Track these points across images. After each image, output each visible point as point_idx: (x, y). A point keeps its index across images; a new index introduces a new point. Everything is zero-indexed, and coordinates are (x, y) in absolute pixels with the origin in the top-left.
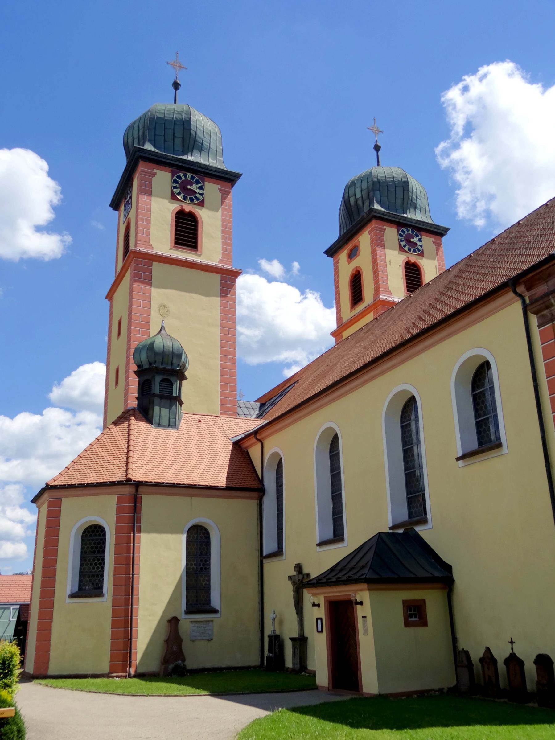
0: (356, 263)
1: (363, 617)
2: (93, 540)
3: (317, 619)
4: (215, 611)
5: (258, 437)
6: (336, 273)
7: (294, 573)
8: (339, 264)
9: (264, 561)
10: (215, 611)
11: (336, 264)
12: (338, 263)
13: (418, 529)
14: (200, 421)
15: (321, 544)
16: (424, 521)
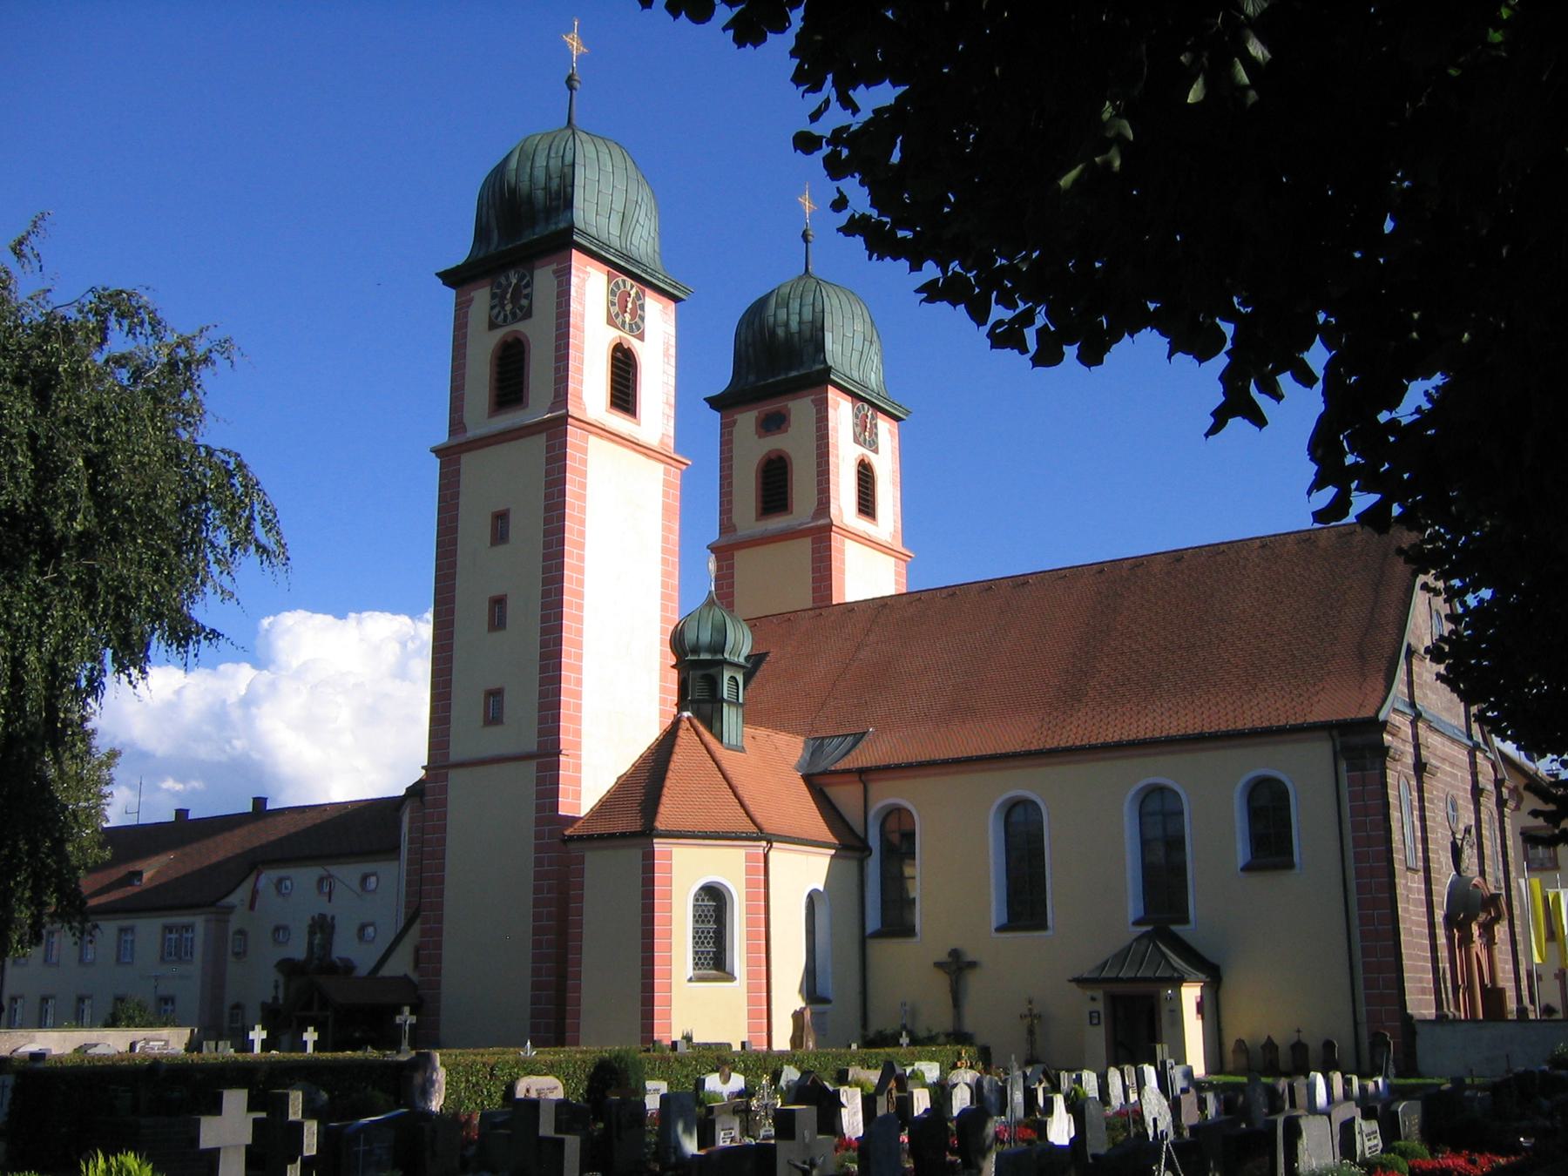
2: (706, 906)
3: (1091, 1013)
7: (950, 960)
8: (736, 430)
11: (727, 429)
15: (999, 929)
16: (1185, 920)
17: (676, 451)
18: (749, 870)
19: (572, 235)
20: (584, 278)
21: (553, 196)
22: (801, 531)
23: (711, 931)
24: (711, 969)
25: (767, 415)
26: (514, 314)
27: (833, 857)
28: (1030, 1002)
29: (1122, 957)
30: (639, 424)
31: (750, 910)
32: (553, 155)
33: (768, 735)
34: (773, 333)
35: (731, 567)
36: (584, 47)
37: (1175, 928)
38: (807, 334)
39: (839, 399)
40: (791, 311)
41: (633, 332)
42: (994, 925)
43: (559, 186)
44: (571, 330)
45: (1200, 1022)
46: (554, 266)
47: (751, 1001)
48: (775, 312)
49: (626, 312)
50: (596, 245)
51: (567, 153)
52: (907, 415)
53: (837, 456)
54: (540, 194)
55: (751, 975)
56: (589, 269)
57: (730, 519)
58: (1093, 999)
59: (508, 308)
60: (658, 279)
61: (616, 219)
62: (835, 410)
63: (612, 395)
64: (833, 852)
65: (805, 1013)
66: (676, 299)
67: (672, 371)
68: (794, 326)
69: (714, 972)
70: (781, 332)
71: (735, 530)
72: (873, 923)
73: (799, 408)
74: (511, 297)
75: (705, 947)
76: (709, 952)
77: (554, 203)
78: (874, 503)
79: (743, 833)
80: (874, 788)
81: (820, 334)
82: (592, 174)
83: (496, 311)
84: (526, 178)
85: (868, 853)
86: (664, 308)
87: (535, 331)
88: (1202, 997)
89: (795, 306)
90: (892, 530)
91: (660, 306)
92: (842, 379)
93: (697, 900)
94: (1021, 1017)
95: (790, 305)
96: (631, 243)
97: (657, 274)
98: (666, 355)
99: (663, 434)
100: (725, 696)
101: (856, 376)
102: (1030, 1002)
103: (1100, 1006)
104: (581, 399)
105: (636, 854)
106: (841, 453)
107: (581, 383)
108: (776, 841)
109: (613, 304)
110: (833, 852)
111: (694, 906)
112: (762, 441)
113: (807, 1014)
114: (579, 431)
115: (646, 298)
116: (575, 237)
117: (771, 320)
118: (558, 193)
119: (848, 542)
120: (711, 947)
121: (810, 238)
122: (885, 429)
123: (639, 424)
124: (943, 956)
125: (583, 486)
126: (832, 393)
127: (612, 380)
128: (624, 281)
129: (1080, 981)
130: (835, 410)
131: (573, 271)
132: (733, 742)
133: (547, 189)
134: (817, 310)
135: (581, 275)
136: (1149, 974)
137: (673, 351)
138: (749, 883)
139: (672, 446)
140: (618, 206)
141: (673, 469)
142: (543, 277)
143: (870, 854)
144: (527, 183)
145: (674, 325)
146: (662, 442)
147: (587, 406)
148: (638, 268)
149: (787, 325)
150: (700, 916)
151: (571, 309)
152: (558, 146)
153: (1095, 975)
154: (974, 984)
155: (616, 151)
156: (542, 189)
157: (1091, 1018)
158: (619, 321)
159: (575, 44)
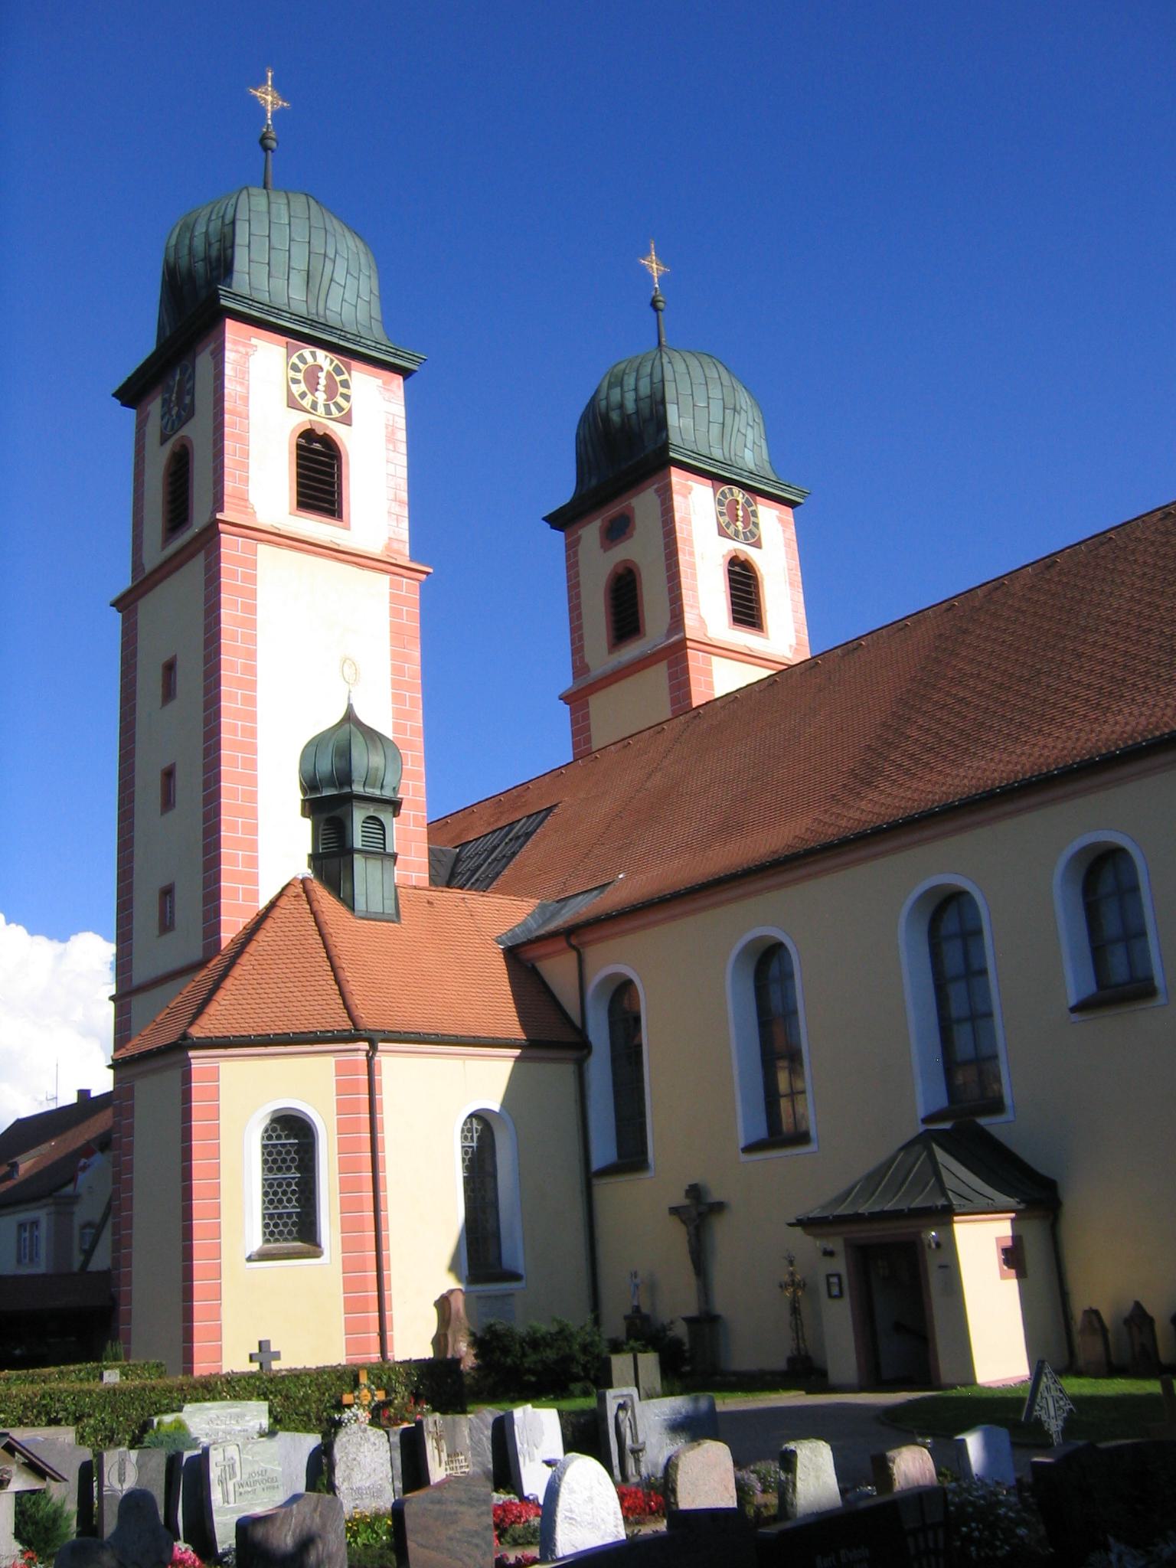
0: (623, 552)
1: (941, 1267)
2: (284, 1145)
3: (828, 1276)
4: (515, 1277)
5: (574, 942)
6: (572, 565)
7: (686, 1202)
9: (595, 1181)
10: (515, 1277)
11: (572, 547)
12: (577, 545)
13: (983, 1121)
14: (429, 902)
15: (749, 1149)
17: (412, 559)
18: (342, 1088)
19: (219, 301)
20: (247, 354)
21: (214, 265)
22: (654, 654)
23: (293, 1182)
24: (294, 1239)
25: (610, 521)
26: (178, 415)
27: (518, 1059)
28: (791, 1263)
29: (873, 1180)
30: (347, 528)
31: (344, 1147)
32: (213, 217)
33: (464, 898)
34: (606, 419)
35: (586, 717)
36: (284, 101)
37: (983, 1121)
38: (646, 412)
39: (690, 483)
40: (626, 388)
41: (331, 414)
42: (742, 1143)
43: (219, 250)
44: (227, 416)
45: (1012, 1285)
46: (212, 347)
47: (349, 1285)
48: (608, 394)
49: (317, 390)
50: (260, 310)
51: (229, 209)
52: (803, 497)
53: (692, 554)
54: (200, 266)
55: (347, 1246)
56: (254, 341)
57: (582, 658)
58: (829, 1253)
59: (174, 412)
60: (367, 347)
61: (298, 280)
62: (685, 496)
63: (299, 494)
64: (517, 1052)
65: (452, 1299)
66: (405, 373)
67: (403, 460)
68: (630, 407)
69: (299, 1244)
70: (615, 416)
71: (589, 671)
72: (604, 1151)
73: (643, 503)
74: (177, 398)
75: (285, 1207)
76: (281, 1214)
77: (215, 273)
78: (759, 610)
79: (328, 1031)
80: (592, 954)
81: (661, 407)
82: (260, 228)
83: (165, 420)
84: (185, 251)
85: (585, 1052)
86: (384, 383)
87: (196, 431)
88: (1016, 1238)
89: (630, 381)
90: (793, 642)
91: (380, 382)
92: (689, 457)
93: (269, 1138)
94: (781, 1286)
95: (625, 383)
96: (326, 308)
97: (363, 340)
98: (391, 439)
99: (390, 539)
100: (358, 843)
101: (717, 454)
102: (791, 1263)
103: (839, 1265)
104: (247, 500)
105: (176, 1074)
106: (697, 548)
107: (246, 481)
108: (383, 1041)
109: (296, 381)
110: (517, 1052)
111: (264, 1147)
112: (610, 553)
113: (458, 1303)
114: (241, 539)
115: (353, 373)
116: (222, 301)
117: (603, 403)
118: (218, 259)
119: (714, 659)
120: (294, 1207)
121: (661, 305)
122: (771, 519)
123: (347, 528)
124: (680, 1199)
125: (251, 609)
126: (677, 476)
127: (299, 475)
128: (313, 354)
129: (806, 1224)
130: (685, 496)
131: (228, 345)
132: (376, 907)
133: (207, 259)
134: (655, 381)
135: (242, 350)
136: (903, 1206)
137: (402, 436)
138: (342, 1107)
139: (407, 552)
140: (300, 262)
141: (405, 580)
142: (203, 362)
143: (590, 1052)
144: (186, 258)
145: (403, 403)
146: (388, 547)
147: (256, 509)
148: (331, 334)
149: (621, 406)
150: (275, 1161)
151: (226, 391)
152: (220, 208)
153: (843, 1210)
154: (724, 1235)
155: (299, 202)
156: (202, 260)
157: (829, 1285)
158: (306, 403)
159: (269, 98)
